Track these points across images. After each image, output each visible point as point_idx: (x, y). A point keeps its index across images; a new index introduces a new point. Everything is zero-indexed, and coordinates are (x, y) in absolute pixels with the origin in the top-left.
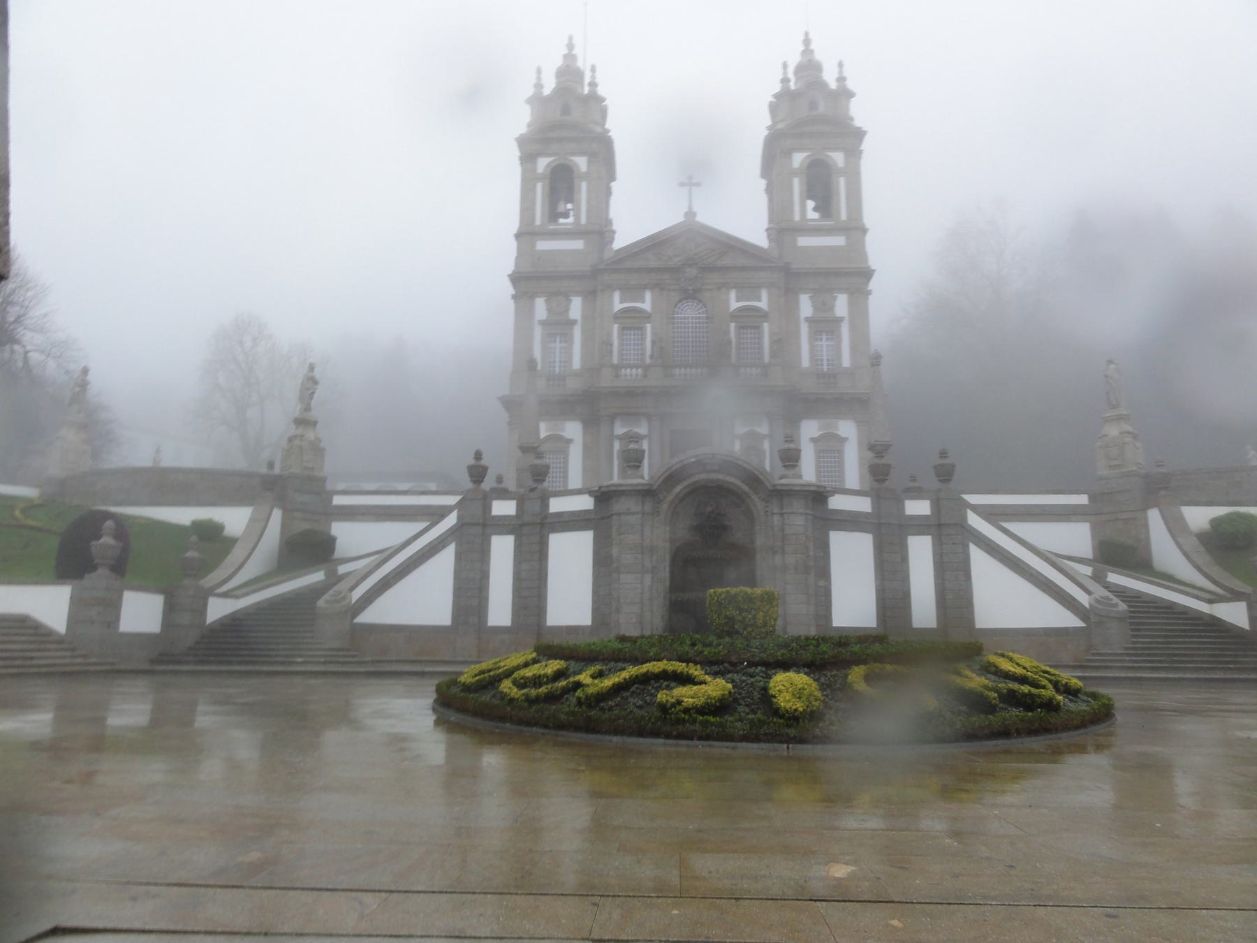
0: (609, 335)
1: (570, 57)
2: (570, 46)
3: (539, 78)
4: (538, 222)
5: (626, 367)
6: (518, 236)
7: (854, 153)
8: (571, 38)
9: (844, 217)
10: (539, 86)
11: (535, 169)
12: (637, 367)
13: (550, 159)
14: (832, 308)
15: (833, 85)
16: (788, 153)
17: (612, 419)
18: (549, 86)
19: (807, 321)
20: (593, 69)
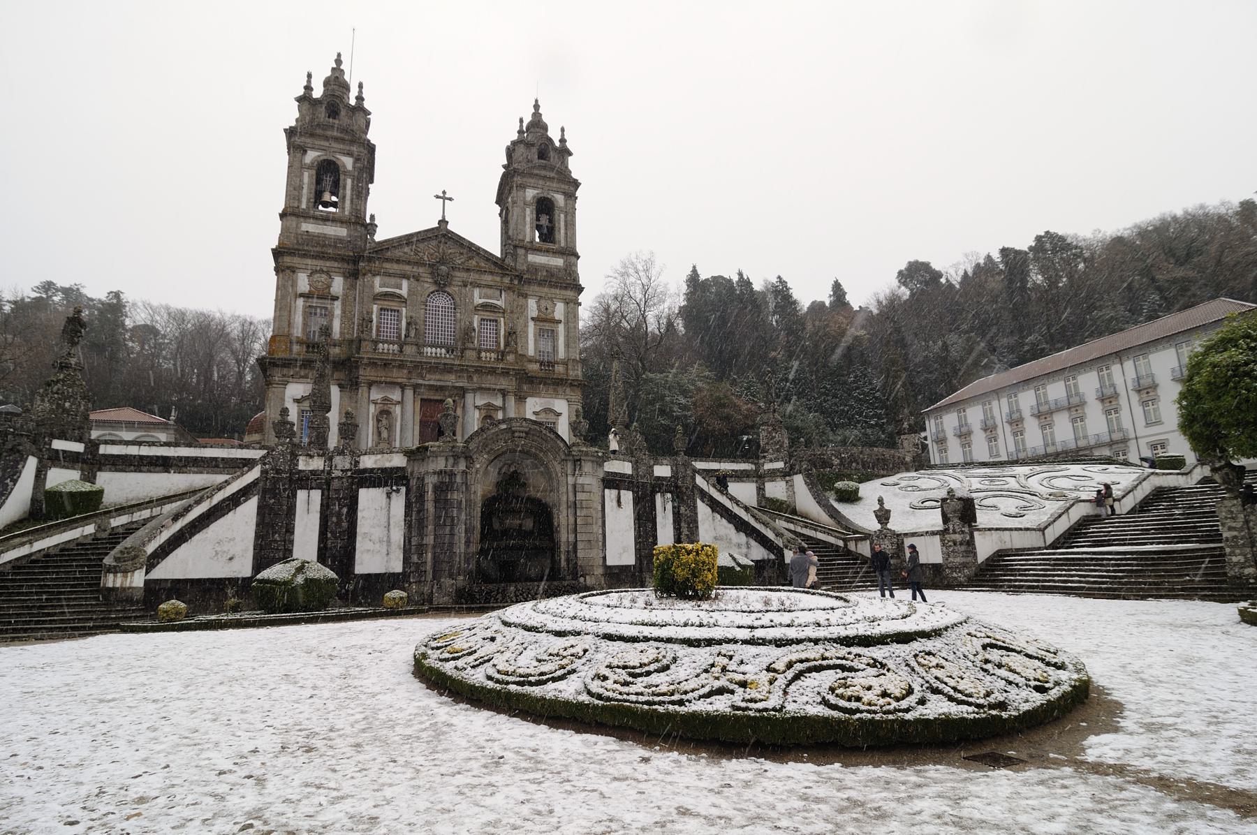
0: (370, 313)
1: (337, 72)
2: (338, 61)
3: (309, 81)
4: (304, 206)
5: (384, 342)
6: (283, 216)
7: (571, 197)
8: (339, 55)
10: (308, 88)
12: (393, 343)
14: (553, 312)
15: (557, 144)
16: (523, 187)
17: (370, 384)
18: (318, 92)
20: (361, 86)
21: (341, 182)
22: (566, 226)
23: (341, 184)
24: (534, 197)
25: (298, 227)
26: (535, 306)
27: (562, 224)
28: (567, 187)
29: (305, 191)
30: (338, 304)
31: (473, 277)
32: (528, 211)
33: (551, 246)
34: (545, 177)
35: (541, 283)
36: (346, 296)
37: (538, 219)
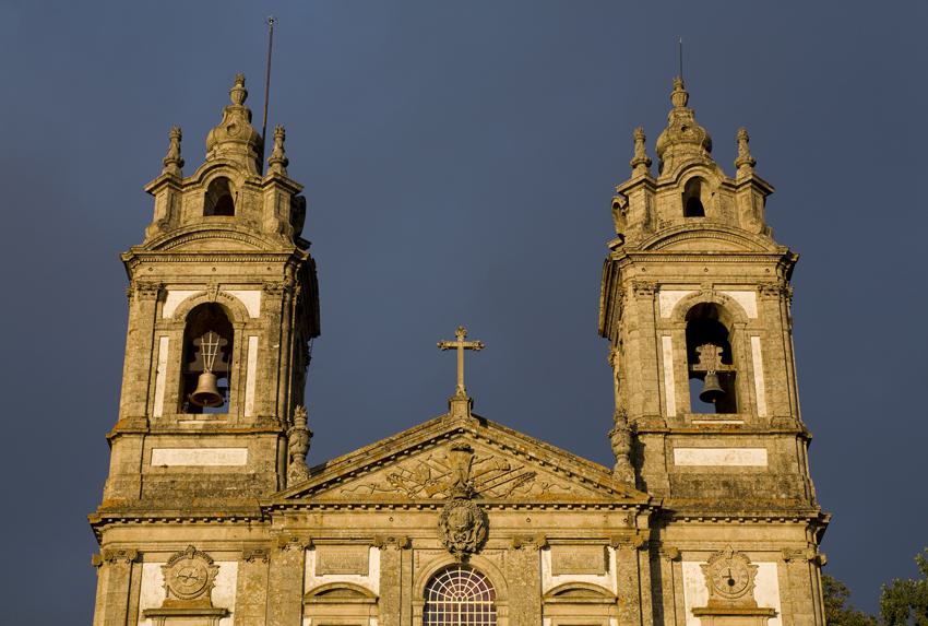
13: (188, 294)
14: (749, 587)
19: (696, 615)
21: (237, 343)
22: (766, 363)
23: (236, 353)
24: (677, 309)
26: (701, 578)
27: (757, 360)
28: (760, 270)
29: (161, 379)
31: (541, 521)
32: (667, 343)
33: (729, 420)
34: (704, 254)
35: (708, 514)
36: (240, 601)
37: (693, 358)
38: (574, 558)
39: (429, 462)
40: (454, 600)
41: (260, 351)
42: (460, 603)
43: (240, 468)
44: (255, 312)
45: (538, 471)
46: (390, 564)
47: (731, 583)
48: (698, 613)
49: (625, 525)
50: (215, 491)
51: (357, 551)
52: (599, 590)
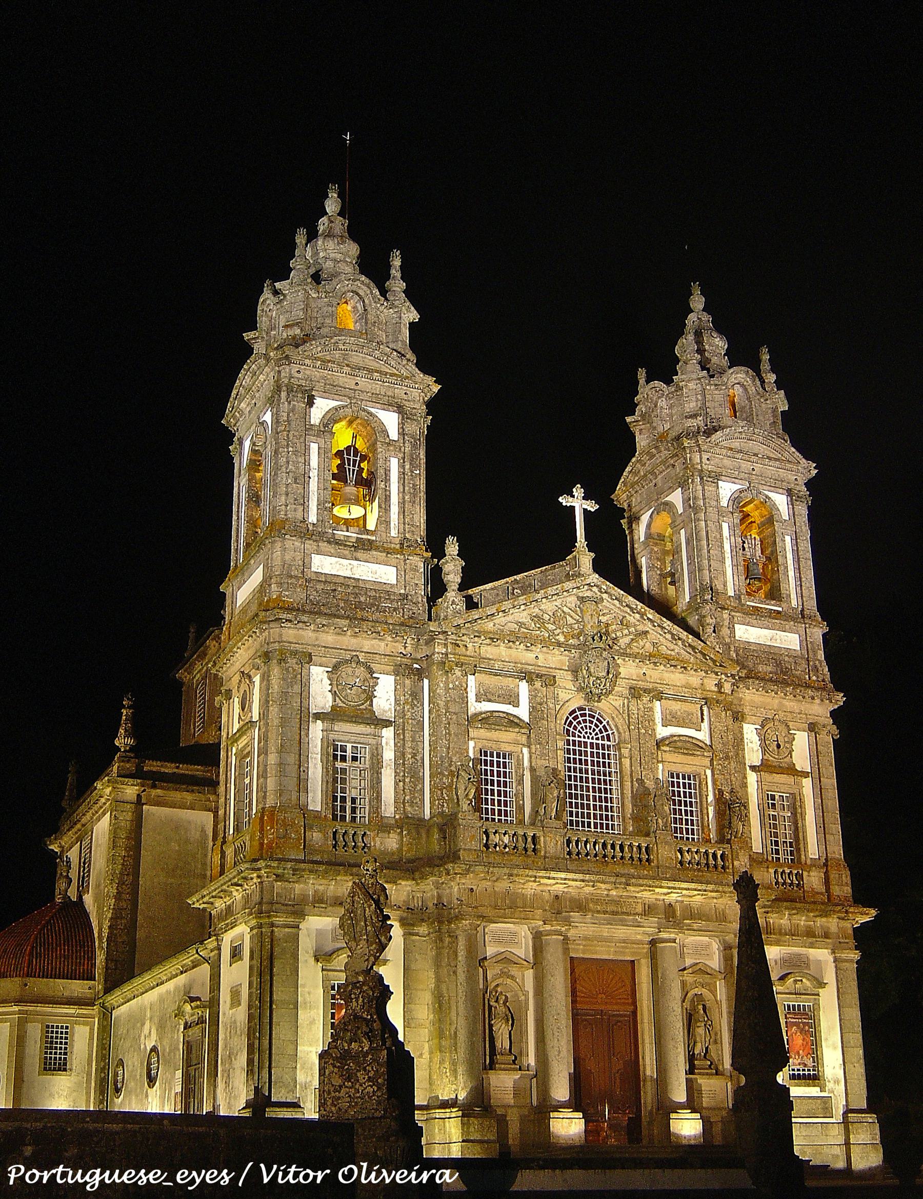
4: (313, 518)
9: (794, 603)
11: (306, 416)
25: (306, 564)
26: (756, 739)
27: (790, 556)
29: (313, 485)
30: (388, 733)
36: (400, 714)
38: (679, 713)
39: (565, 609)
40: (584, 737)
41: (402, 475)
42: (589, 741)
43: (392, 586)
44: (394, 434)
45: (651, 631)
46: (538, 699)
47: (778, 746)
48: (753, 768)
49: (716, 689)
50: (373, 605)
51: (509, 682)
52: (700, 744)
